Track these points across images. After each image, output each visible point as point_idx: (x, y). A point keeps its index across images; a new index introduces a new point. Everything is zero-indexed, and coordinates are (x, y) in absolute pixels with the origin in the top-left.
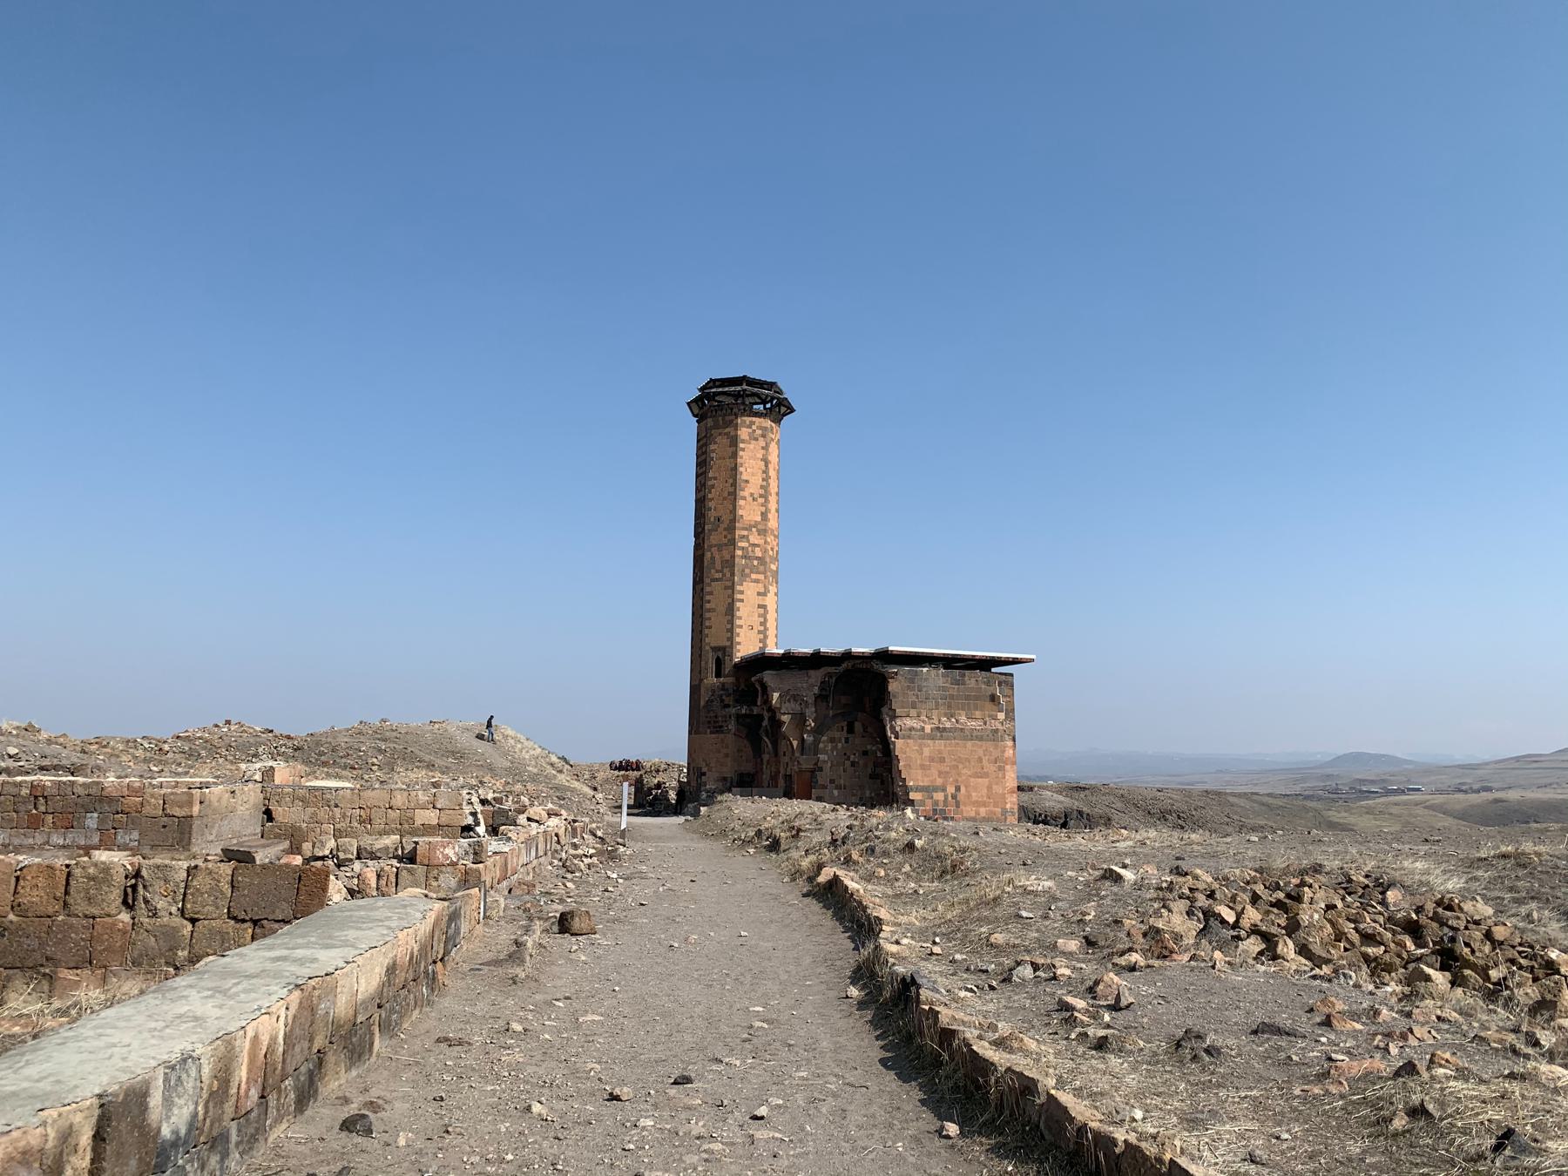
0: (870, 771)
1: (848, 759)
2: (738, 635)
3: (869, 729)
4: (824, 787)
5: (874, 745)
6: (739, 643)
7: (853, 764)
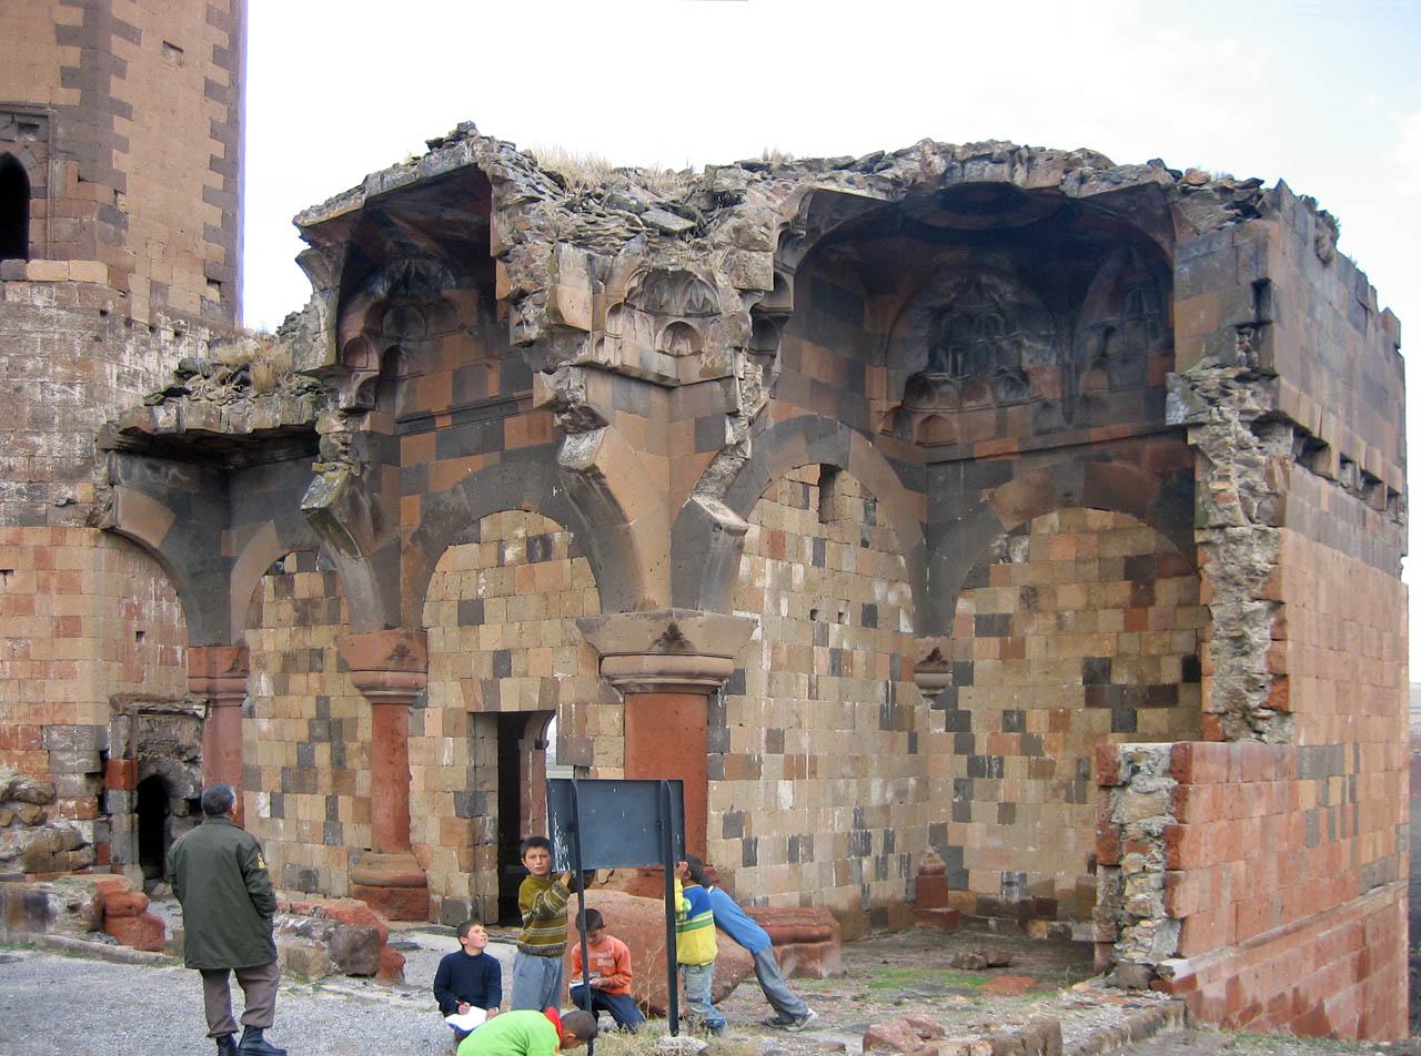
0: (880, 692)
1: (825, 642)
2: (120, 69)
3: (880, 515)
4: (750, 769)
5: (892, 582)
6: (125, 110)
7: (839, 662)
